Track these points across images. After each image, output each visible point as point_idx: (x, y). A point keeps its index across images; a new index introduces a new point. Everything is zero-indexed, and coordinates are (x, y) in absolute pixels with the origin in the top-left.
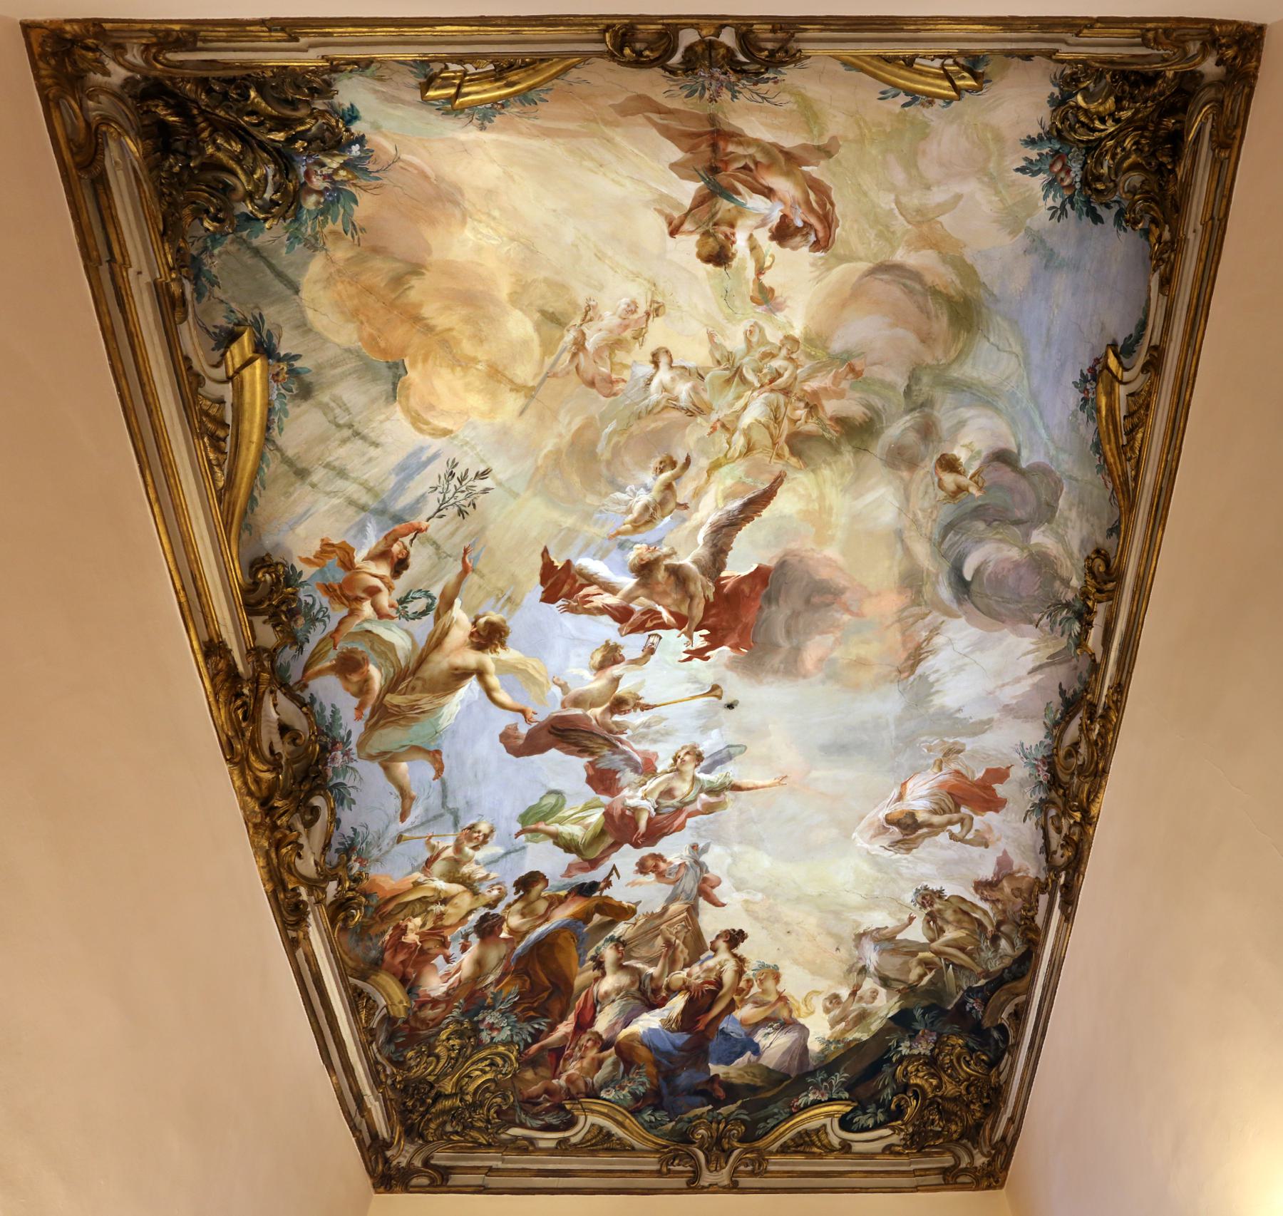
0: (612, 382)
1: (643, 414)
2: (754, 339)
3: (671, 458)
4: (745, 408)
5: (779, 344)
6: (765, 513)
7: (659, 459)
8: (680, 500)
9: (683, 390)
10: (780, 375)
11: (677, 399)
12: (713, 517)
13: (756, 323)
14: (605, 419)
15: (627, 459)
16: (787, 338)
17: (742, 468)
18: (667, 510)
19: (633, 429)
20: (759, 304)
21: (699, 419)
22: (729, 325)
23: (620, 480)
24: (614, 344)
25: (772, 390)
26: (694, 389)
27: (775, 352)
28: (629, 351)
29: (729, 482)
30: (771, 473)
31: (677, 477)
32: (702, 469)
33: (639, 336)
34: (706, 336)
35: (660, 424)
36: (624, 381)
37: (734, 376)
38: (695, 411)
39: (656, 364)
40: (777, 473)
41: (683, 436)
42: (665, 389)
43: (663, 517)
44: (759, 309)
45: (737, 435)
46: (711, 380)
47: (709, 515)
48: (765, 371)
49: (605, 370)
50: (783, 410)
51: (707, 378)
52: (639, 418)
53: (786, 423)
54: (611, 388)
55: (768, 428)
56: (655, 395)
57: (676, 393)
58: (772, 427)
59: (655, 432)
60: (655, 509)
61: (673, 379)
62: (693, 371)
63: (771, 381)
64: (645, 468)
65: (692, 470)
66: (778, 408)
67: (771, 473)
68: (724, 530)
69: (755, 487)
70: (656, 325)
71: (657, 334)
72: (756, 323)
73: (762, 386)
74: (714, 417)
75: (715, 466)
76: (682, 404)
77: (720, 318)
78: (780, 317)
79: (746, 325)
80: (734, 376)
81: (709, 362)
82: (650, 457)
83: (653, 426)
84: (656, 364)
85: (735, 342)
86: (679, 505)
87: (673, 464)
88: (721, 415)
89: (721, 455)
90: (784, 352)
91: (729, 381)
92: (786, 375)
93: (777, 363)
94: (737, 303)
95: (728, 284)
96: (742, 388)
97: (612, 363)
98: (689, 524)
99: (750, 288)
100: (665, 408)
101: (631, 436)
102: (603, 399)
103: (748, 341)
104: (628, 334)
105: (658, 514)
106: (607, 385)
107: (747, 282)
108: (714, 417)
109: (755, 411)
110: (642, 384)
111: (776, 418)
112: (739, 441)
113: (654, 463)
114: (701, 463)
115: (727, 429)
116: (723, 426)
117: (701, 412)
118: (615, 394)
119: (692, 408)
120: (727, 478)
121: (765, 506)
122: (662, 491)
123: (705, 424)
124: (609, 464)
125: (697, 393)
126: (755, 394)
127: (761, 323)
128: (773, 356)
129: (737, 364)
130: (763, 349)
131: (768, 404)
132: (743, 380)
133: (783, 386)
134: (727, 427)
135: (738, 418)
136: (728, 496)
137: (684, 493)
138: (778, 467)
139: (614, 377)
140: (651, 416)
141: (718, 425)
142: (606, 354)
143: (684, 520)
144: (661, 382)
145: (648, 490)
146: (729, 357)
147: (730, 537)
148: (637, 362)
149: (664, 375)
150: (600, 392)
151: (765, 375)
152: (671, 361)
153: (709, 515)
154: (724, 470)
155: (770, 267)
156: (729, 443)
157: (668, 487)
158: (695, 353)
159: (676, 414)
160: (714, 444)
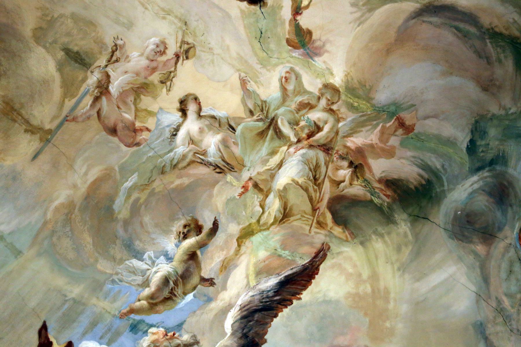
0: (135, 131)
1: (168, 169)
2: (290, 87)
3: (196, 221)
4: (280, 165)
5: (317, 93)
6: (306, 295)
7: (183, 222)
8: (205, 274)
9: (212, 143)
10: (319, 129)
11: (204, 153)
12: (244, 299)
13: (292, 69)
14: (125, 171)
15: (147, 219)
16: (327, 86)
17: (277, 237)
18: (189, 286)
19: (155, 184)
20: (295, 47)
21: (229, 177)
22: (264, 71)
23: (138, 245)
24: (140, 89)
25: (311, 146)
26: (224, 142)
27: (313, 102)
28: (155, 97)
29: (262, 254)
30: (311, 244)
31: (202, 245)
32: (231, 236)
33: (167, 80)
34: (238, 83)
35: (186, 181)
36: (148, 130)
37: (268, 128)
38: (225, 167)
39: (184, 112)
40: (318, 246)
41: (211, 196)
42: (192, 141)
43: (185, 294)
44: (296, 54)
45: (271, 196)
46: (242, 133)
47: (238, 296)
48: (302, 123)
49: (128, 116)
50: (323, 169)
51: (239, 129)
52: (163, 172)
53: (327, 185)
54: (134, 138)
55: (306, 190)
56: (181, 147)
57: (204, 146)
58: (311, 189)
59: (181, 190)
60: (176, 283)
61: (201, 131)
62: (224, 121)
63: (310, 135)
64: (167, 232)
65: (220, 237)
66: (317, 167)
67: (311, 244)
68: (257, 316)
69: (294, 261)
70: (186, 68)
71: (187, 79)
72: (292, 69)
73: (299, 141)
74: (246, 175)
75: (247, 234)
76: (211, 159)
77: (253, 61)
78: (319, 62)
79: (280, 71)
80: (268, 128)
81: (241, 113)
82: (173, 219)
83: (178, 182)
84: (184, 112)
85: (269, 90)
86: (203, 280)
87: (199, 229)
88: (253, 173)
89: (254, 221)
90: (323, 102)
91: (262, 134)
92: (326, 129)
93: (316, 115)
94: (272, 46)
95: (263, 24)
96: (277, 143)
97: (137, 110)
98: (216, 306)
99: (286, 30)
100: (192, 162)
101: (152, 193)
102: (124, 148)
103: (284, 89)
104: (155, 78)
105: (179, 291)
106: (129, 134)
107: (283, 23)
108: (246, 175)
109: (291, 171)
110: (167, 134)
111: (315, 179)
112: (274, 205)
113: (178, 226)
114: (231, 229)
115: (260, 190)
116: (256, 186)
117: (231, 169)
118: (138, 144)
119: (221, 164)
120: (261, 249)
121: (305, 287)
122: (186, 261)
123: (235, 183)
124: (126, 223)
125: (227, 147)
126: (292, 150)
127: (297, 69)
128: (310, 107)
129: (271, 115)
130: (299, 99)
131: (306, 162)
132: (279, 134)
133: (322, 142)
134: (261, 187)
135: (273, 176)
136: (262, 272)
137: (209, 266)
138: (319, 238)
139: (138, 124)
140: (176, 171)
141: (250, 184)
142: (131, 99)
143: (210, 300)
144: (188, 133)
145: (169, 259)
146: (263, 106)
147: (264, 325)
148: (163, 109)
149: (192, 125)
150: (121, 140)
151: (302, 128)
152: (200, 109)
153: (238, 296)
154: (257, 238)
155: (307, 7)
156: (262, 206)
157: (192, 256)
158: (225, 102)
159: (203, 170)
160: (245, 206)
